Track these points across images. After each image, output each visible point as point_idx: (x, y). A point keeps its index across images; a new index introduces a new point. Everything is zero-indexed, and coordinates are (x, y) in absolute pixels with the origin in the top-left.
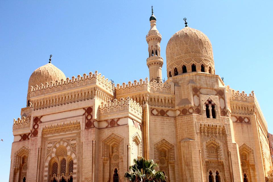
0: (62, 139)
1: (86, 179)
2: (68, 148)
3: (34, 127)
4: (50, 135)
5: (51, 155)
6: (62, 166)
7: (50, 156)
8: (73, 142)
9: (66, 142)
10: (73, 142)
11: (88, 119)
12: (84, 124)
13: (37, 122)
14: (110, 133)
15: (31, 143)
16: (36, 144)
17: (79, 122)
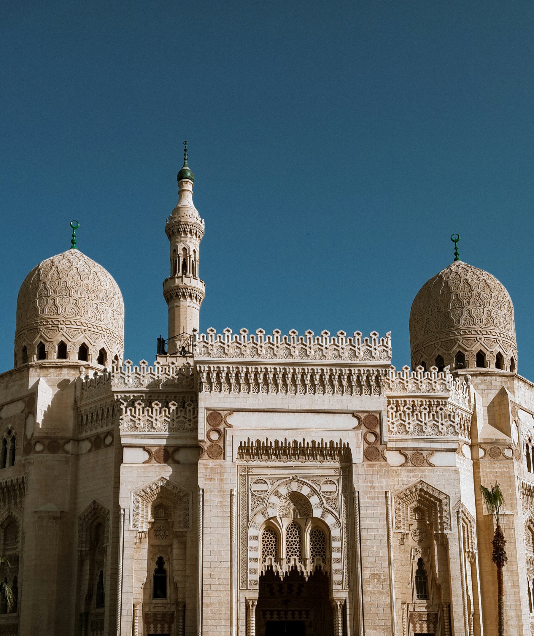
0: (294, 478)
1: (374, 575)
2: (314, 500)
3: (208, 436)
4: (259, 463)
5: (266, 511)
6: (290, 540)
7: (262, 513)
8: (326, 488)
9: (307, 484)
10: (326, 488)
11: (367, 442)
12: (361, 451)
13: (218, 425)
14: (415, 481)
15: (206, 476)
16: (221, 480)
17: (348, 444)
